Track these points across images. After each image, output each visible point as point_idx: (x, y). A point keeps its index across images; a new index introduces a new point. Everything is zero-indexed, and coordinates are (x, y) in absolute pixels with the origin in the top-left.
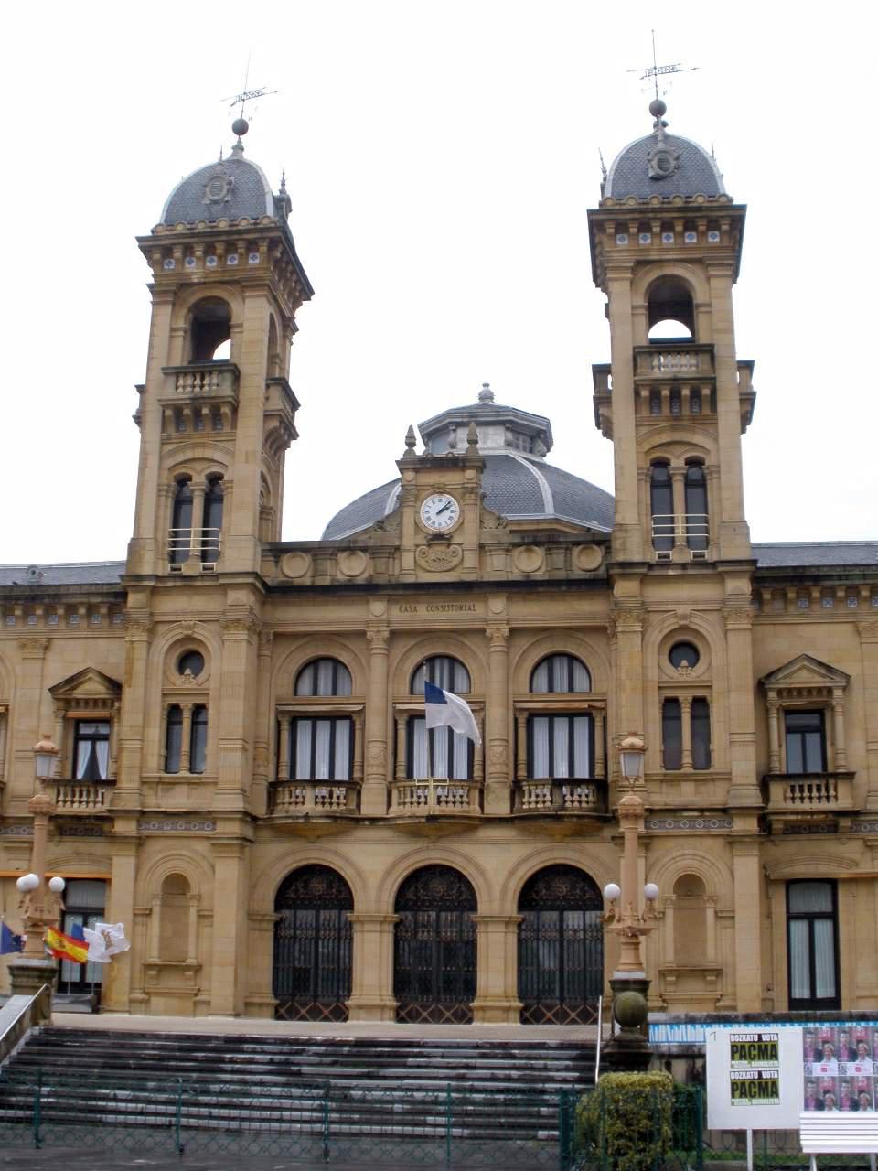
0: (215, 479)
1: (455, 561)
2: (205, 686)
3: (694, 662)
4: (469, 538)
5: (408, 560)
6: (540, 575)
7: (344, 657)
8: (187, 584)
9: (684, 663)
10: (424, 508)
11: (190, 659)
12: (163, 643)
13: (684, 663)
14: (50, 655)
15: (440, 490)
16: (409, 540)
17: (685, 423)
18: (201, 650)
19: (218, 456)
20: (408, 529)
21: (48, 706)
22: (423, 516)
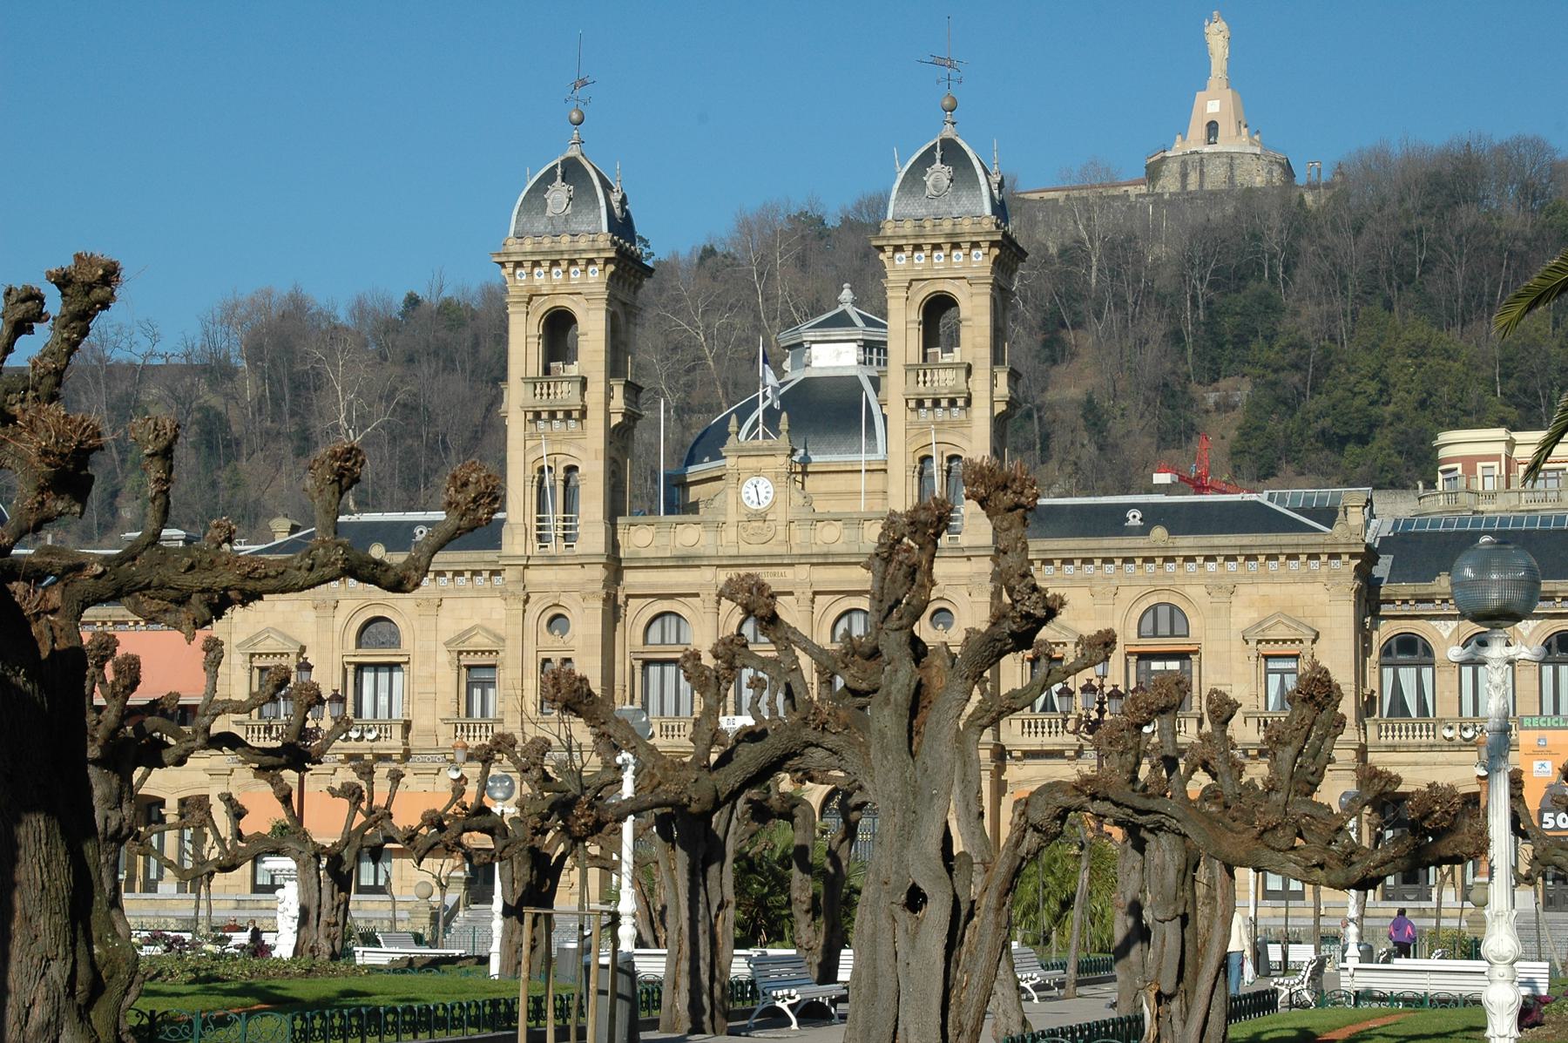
0: (571, 469)
1: (770, 535)
2: (571, 643)
3: (948, 626)
4: (780, 516)
5: (730, 534)
6: (839, 548)
7: (684, 612)
8: (552, 562)
9: (941, 626)
10: (744, 489)
11: (557, 621)
12: (534, 609)
13: (941, 626)
14: (442, 611)
15: (758, 473)
16: (732, 517)
17: (946, 427)
18: (566, 614)
19: (573, 452)
20: (732, 508)
21: (444, 657)
22: (744, 496)
